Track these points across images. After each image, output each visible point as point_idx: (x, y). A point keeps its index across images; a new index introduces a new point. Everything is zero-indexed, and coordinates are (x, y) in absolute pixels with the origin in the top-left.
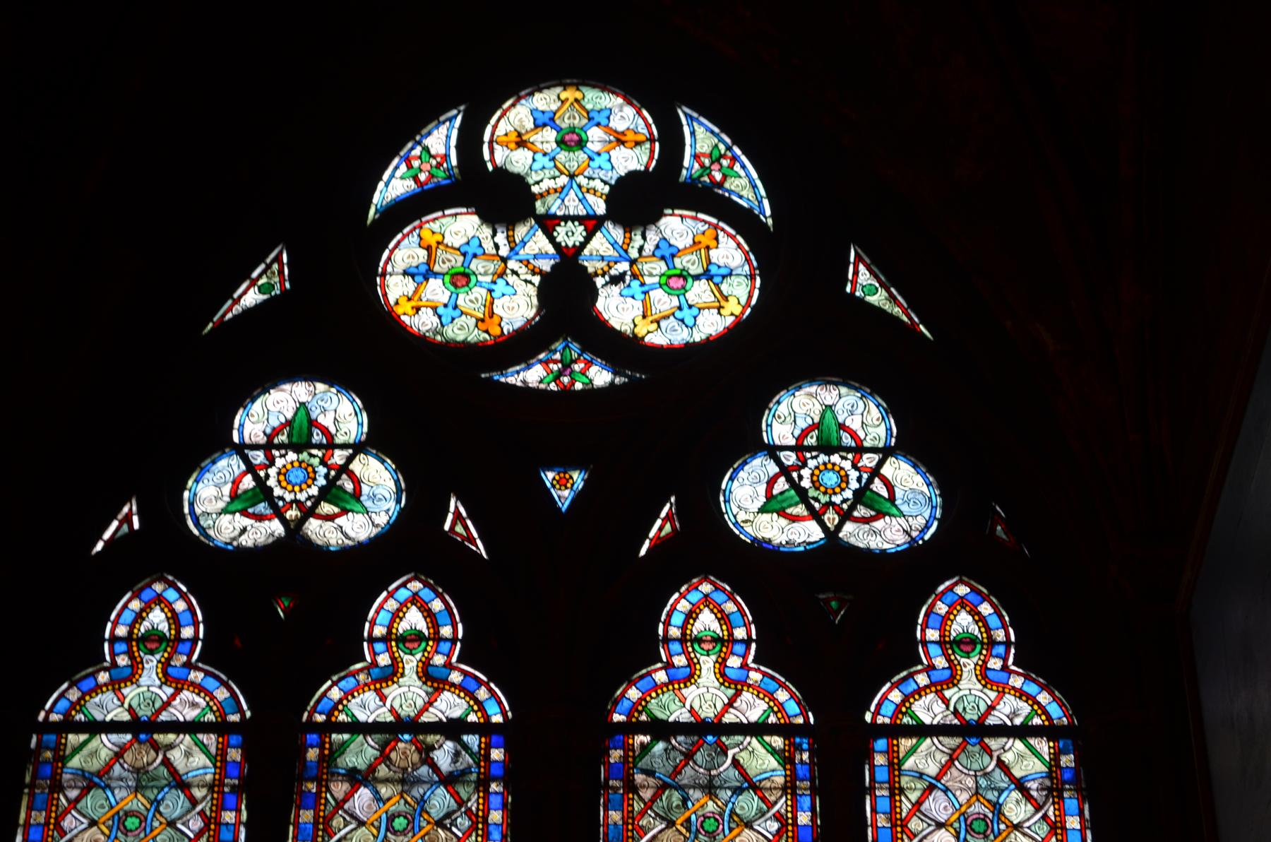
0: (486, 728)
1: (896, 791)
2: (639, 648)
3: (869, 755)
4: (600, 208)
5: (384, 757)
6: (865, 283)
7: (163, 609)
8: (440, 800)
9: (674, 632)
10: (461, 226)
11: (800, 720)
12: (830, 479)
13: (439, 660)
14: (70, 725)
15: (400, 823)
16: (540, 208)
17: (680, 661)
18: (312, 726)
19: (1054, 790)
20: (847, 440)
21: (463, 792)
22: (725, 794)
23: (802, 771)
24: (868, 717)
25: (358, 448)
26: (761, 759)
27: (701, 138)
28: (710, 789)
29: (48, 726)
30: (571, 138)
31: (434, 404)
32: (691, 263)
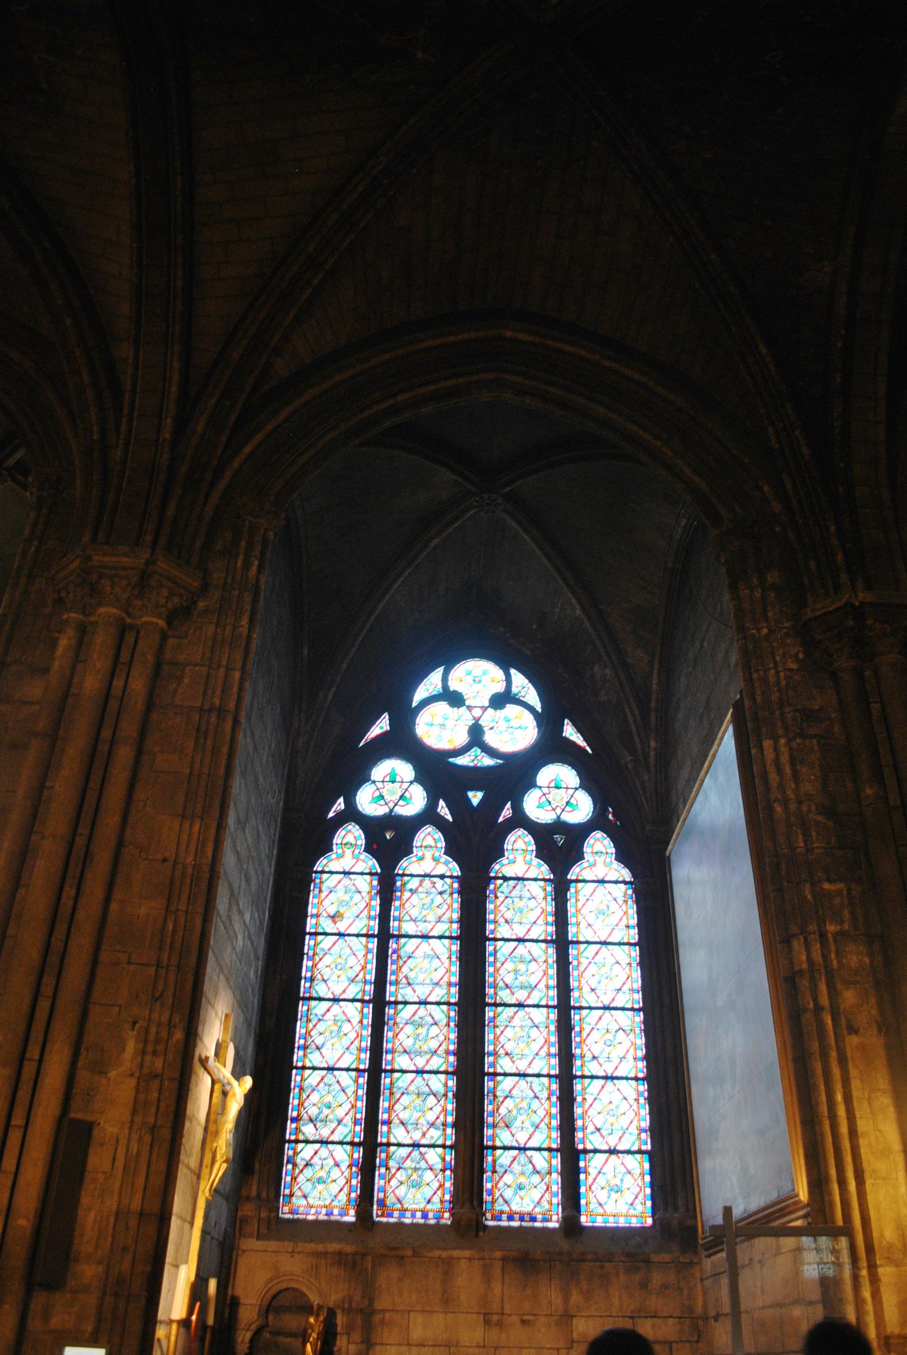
0: (451, 877)
1: (577, 900)
2: (498, 853)
3: (568, 889)
4: (487, 704)
5: (420, 885)
6: (570, 732)
7: (351, 835)
8: (438, 900)
9: (510, 847)
10: (442, 708)
11: (547, 877)
12: (558, 798)
13: (437, 854)
14: (323, 872)
15: (426, 907)
16: (467, 703)
17: (511, 857)
18: (398, 875)
19: (626, 902)
20: (563, 785)
21: (446, 896)
22: (525, 900)
23: (548, 893)
24: (569, 877)
25: (411, 783)
26: (536, 888)
27: (519, 680)
28: (521, 898)
29: (316, 872)
30: (477, 677)
31: (435, 770)
32: (515, 723)
